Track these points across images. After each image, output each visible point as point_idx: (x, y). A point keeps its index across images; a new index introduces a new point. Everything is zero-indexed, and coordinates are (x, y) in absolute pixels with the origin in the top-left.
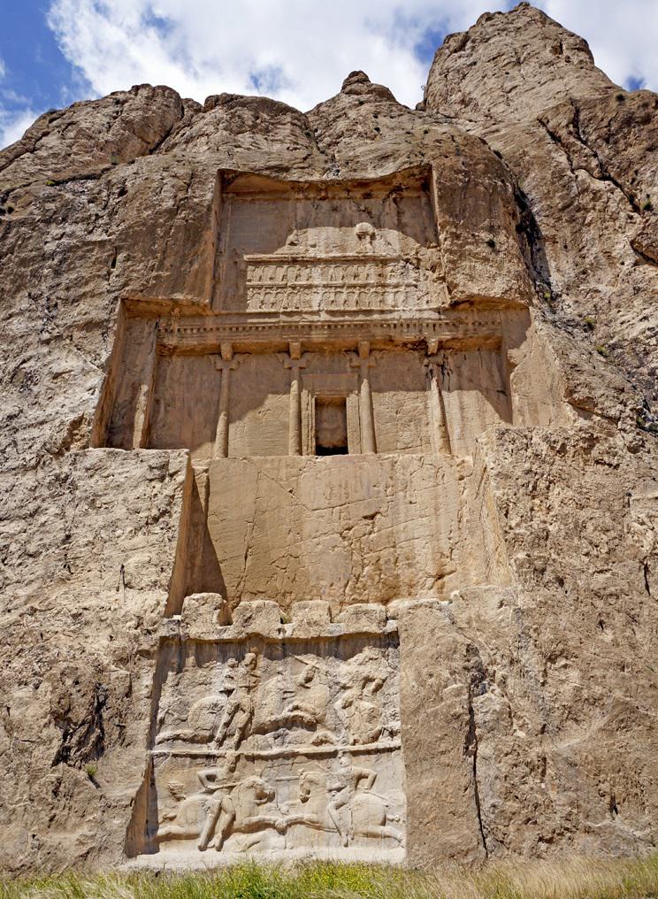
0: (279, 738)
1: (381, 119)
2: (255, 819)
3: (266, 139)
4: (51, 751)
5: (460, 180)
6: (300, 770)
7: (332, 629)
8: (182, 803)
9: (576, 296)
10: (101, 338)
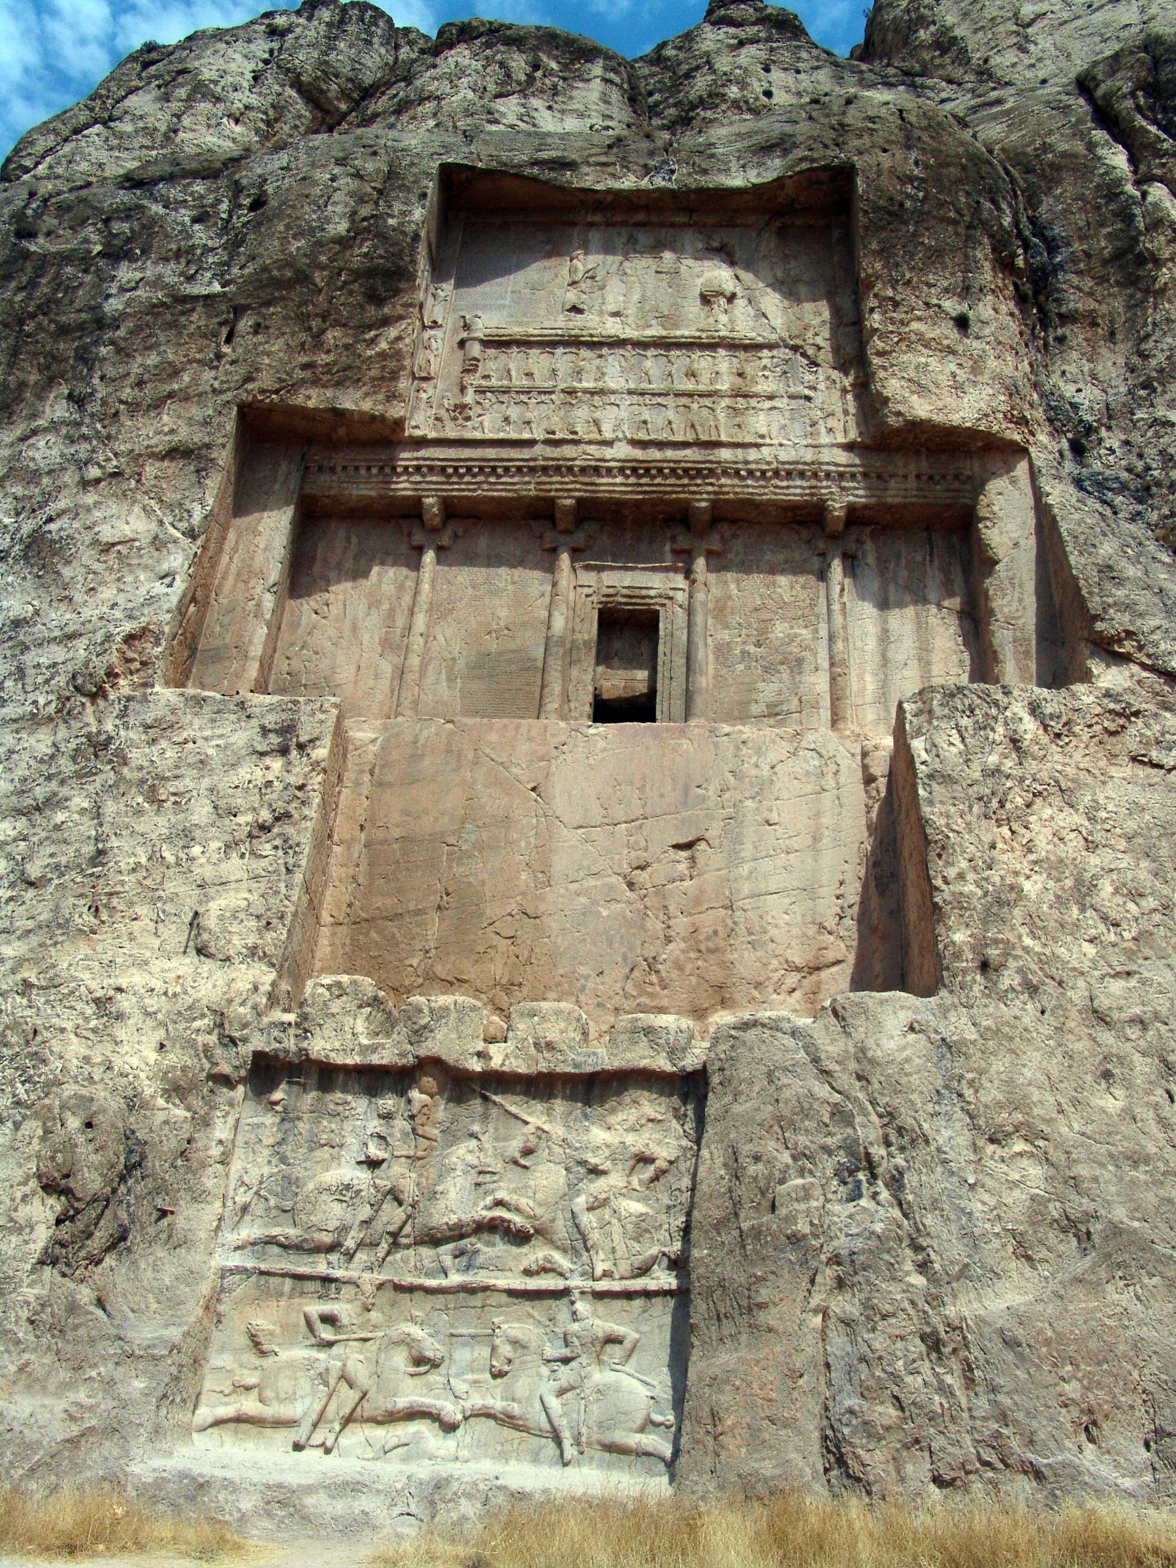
1: (776, 75)
3: (550, 108)
4: (32, 1246)
5: (909, 196)
7: (579, 1059)
8: (268, 1362)
9: (1125, 430)
10: (194, 478)
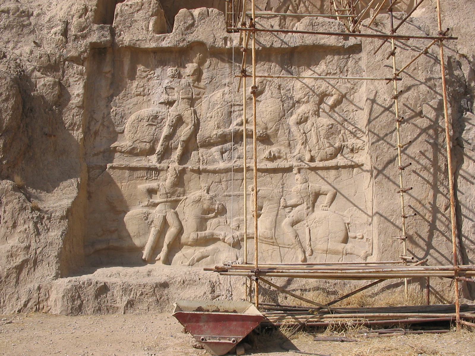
2: (202, 234)
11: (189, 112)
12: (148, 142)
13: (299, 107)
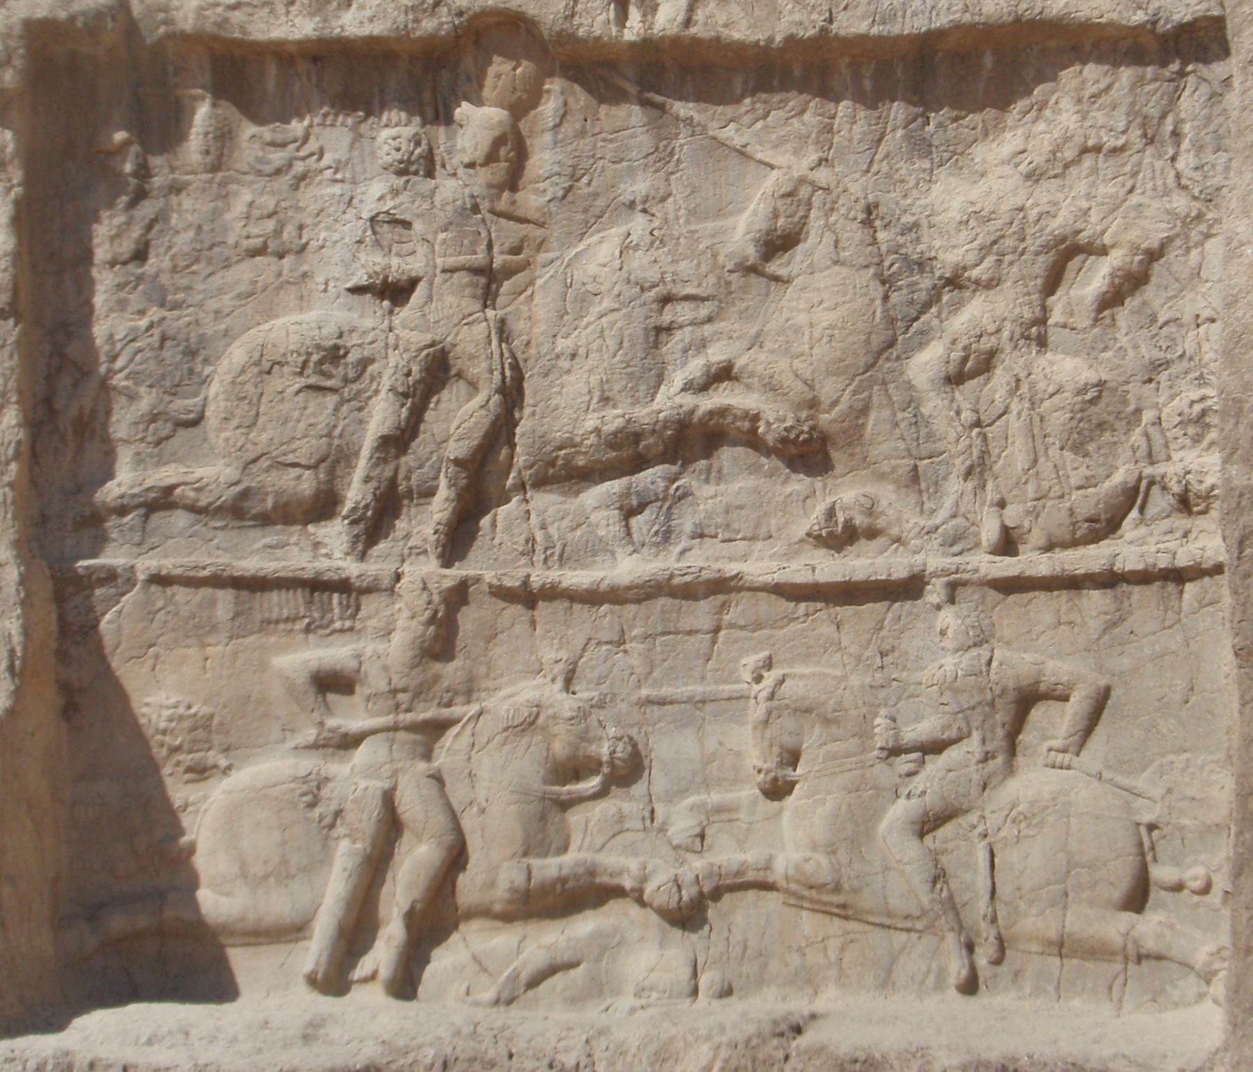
0: (647, 514)
6: (752, 660)
11: (480, 330)
12: (308, 468)
13: (957, 306)
